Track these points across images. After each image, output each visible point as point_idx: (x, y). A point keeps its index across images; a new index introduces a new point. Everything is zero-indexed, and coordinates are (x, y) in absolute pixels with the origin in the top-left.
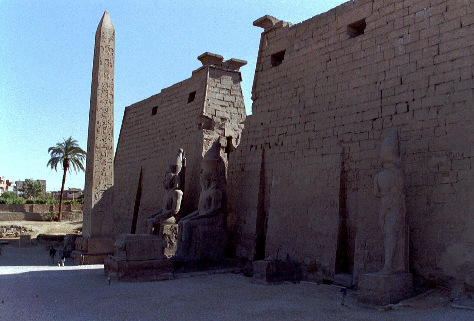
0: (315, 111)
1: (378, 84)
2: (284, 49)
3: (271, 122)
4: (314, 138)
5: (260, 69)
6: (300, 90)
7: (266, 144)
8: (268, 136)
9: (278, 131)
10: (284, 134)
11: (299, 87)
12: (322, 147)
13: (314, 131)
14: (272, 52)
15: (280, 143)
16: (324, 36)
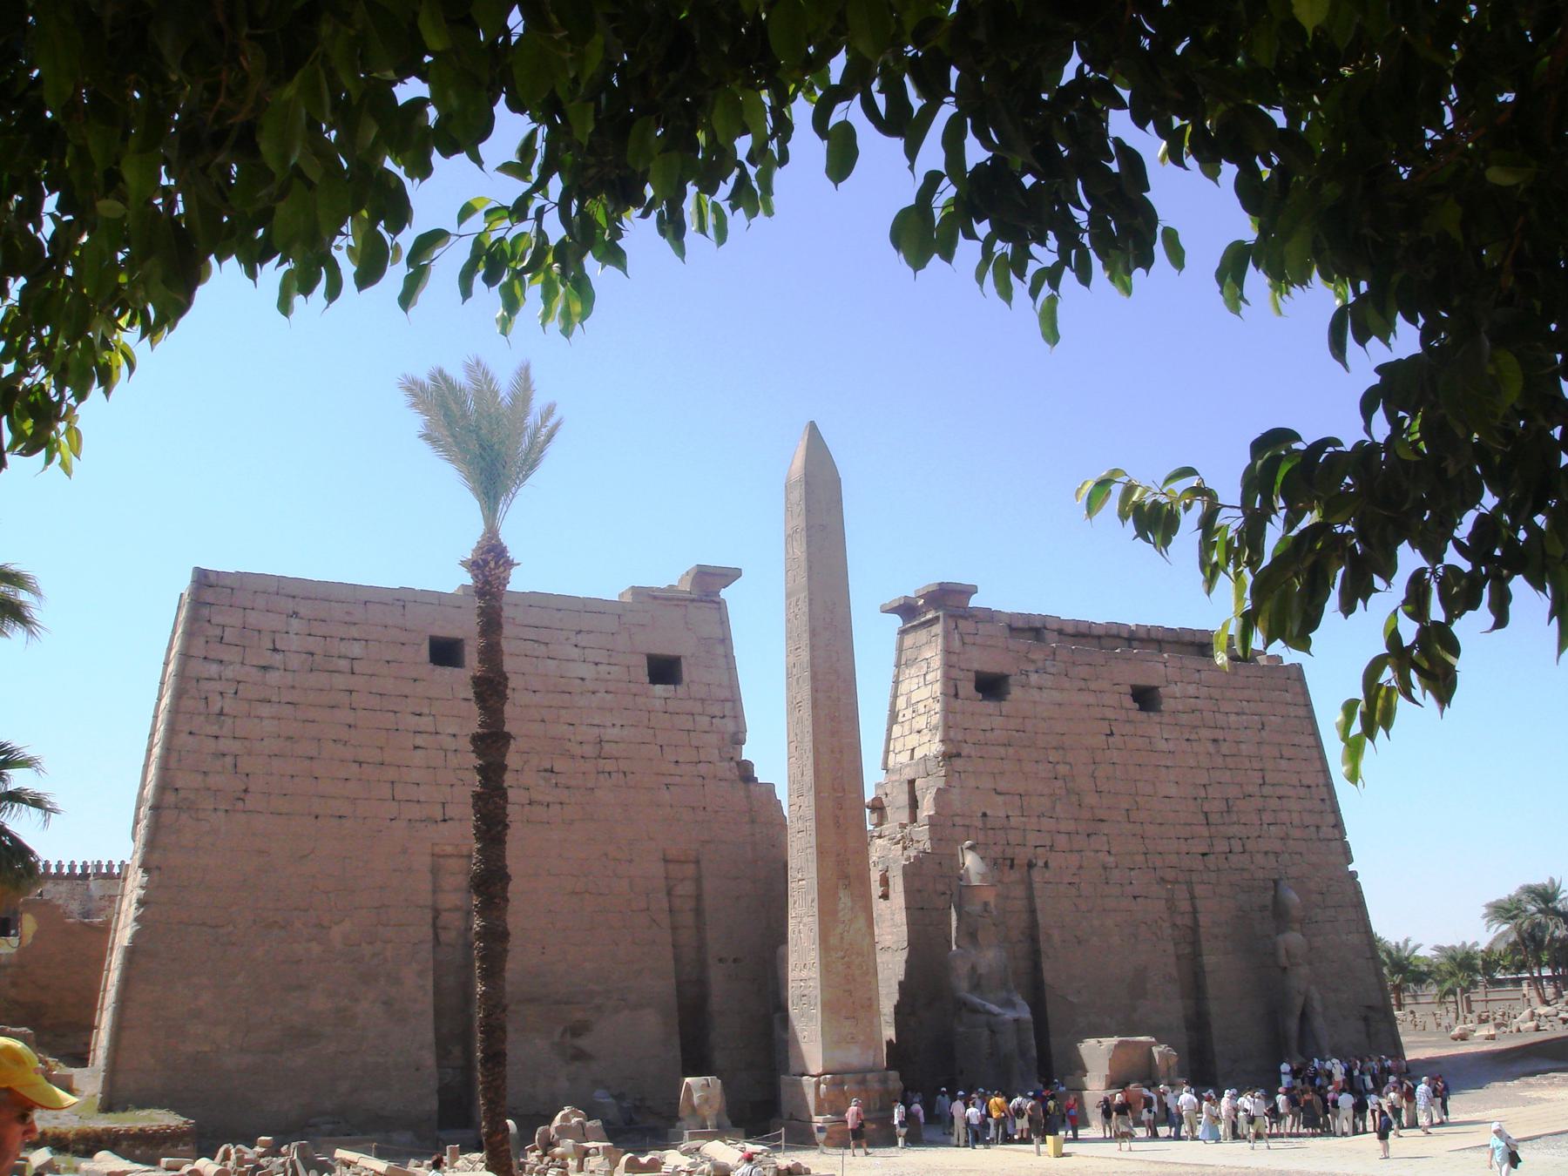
0: (1105, 818)
1: (1199, 801)
2: (1006, 672)
3: (1008, 817)
4: (1113, 865)
5: (952, 692)
6: (1062, 769)
7: (1004, 859)
8: (1008, 844)
9: (1032, 839)
10: (1048, 848)
11: (1058, 763)
12: (1131, 883)
13: (1109, 852)
14: (976, 666)
15: (1041, 863)
16: (1093, 686)
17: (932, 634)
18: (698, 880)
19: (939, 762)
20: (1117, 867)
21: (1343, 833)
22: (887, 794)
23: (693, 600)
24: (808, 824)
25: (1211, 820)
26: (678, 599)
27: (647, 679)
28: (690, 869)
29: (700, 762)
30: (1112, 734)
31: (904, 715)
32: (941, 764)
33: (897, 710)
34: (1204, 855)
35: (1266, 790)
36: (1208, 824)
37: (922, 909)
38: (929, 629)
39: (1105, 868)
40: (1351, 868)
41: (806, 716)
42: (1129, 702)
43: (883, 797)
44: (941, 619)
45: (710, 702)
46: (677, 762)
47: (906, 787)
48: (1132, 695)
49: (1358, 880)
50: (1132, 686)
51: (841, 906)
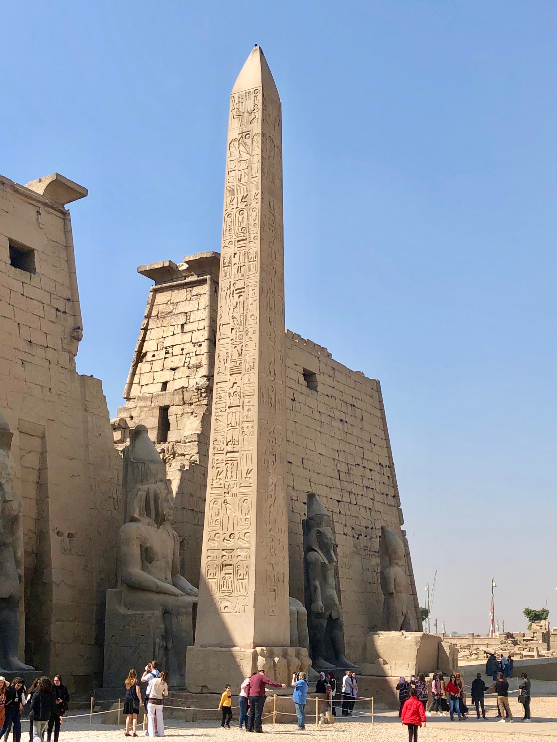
17: (194, 293)
18: (43, 454)
19: (201, 393)
20: (297, 500)
21: (399, 504)
22: (132, 418)
23: (45, 204)
24: (246, 400)
25: (341, 479)
26: (35, 200)
27: (10, 263)
28: (36, 443)
29: (47, 347)
30: (294, 400)
31: (154, 356)
32: (204, 395)
33: (144, 351)
34: (339, 501)
35: (365, 463)
36: (340, 479)
37: (193, 510)
38: (191, 289)
39: (292, 500)
40: (402, 528)
41: (251, 301)
42: (302, 378)
43: (128, 420)
44: (208, 282)
45: (56, 297)
46: (30, 342)
47: (157, 412)
48: (304, 375)
49: (406, 537)
50: (304, 369)
51: (271, 481)
